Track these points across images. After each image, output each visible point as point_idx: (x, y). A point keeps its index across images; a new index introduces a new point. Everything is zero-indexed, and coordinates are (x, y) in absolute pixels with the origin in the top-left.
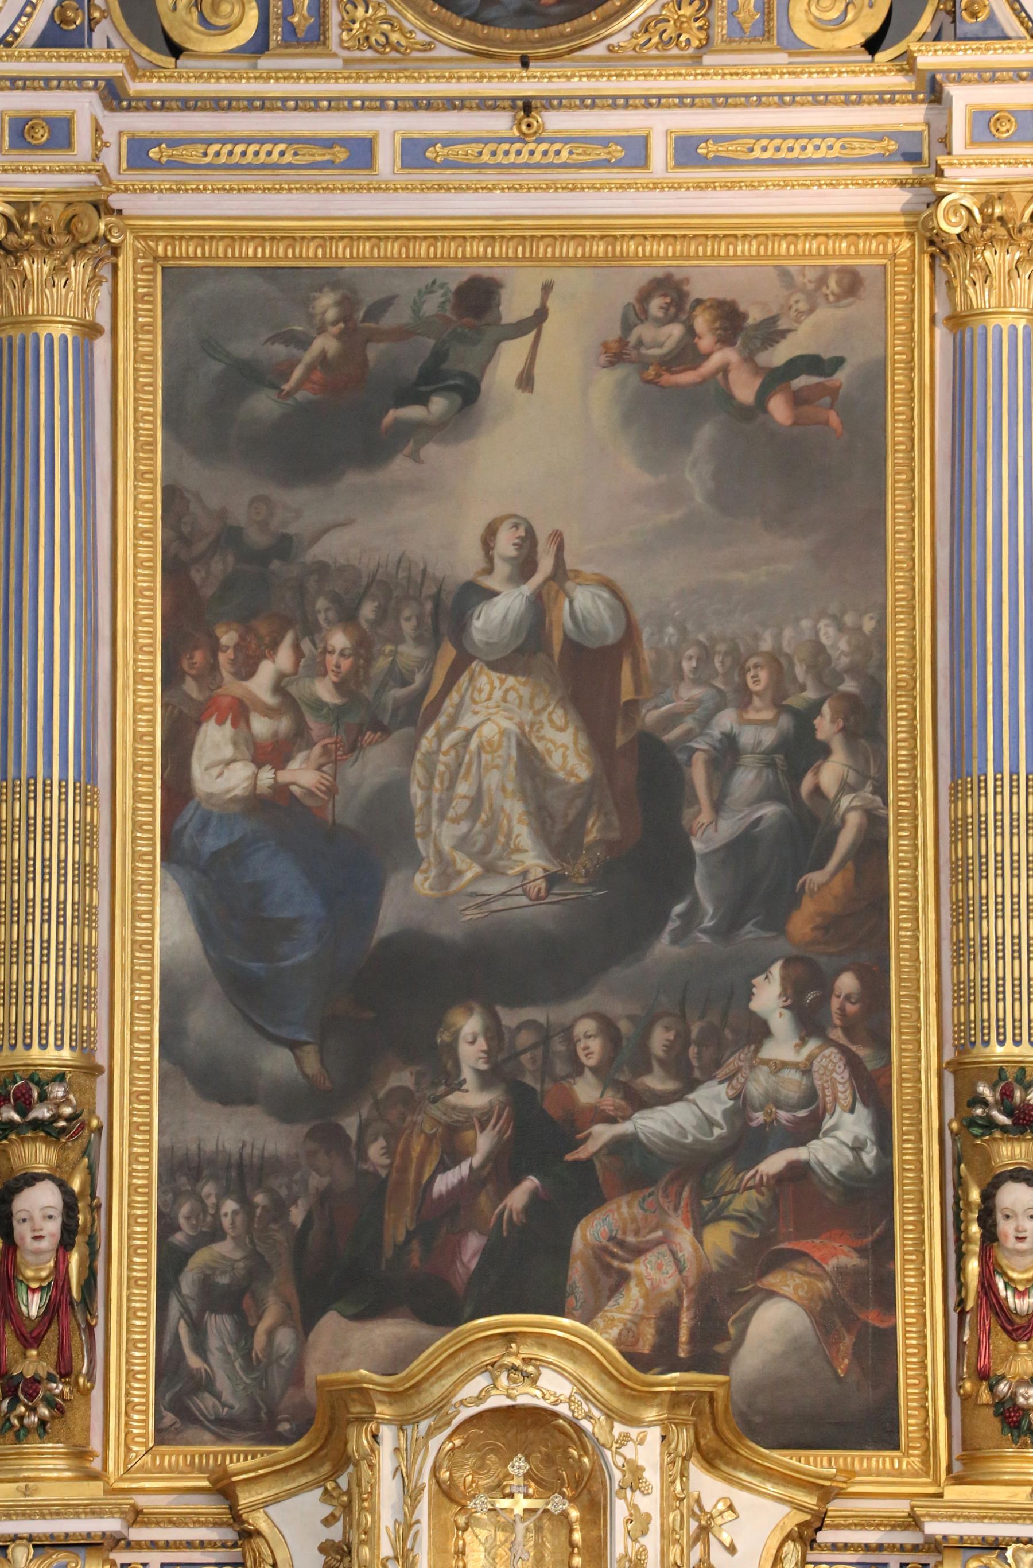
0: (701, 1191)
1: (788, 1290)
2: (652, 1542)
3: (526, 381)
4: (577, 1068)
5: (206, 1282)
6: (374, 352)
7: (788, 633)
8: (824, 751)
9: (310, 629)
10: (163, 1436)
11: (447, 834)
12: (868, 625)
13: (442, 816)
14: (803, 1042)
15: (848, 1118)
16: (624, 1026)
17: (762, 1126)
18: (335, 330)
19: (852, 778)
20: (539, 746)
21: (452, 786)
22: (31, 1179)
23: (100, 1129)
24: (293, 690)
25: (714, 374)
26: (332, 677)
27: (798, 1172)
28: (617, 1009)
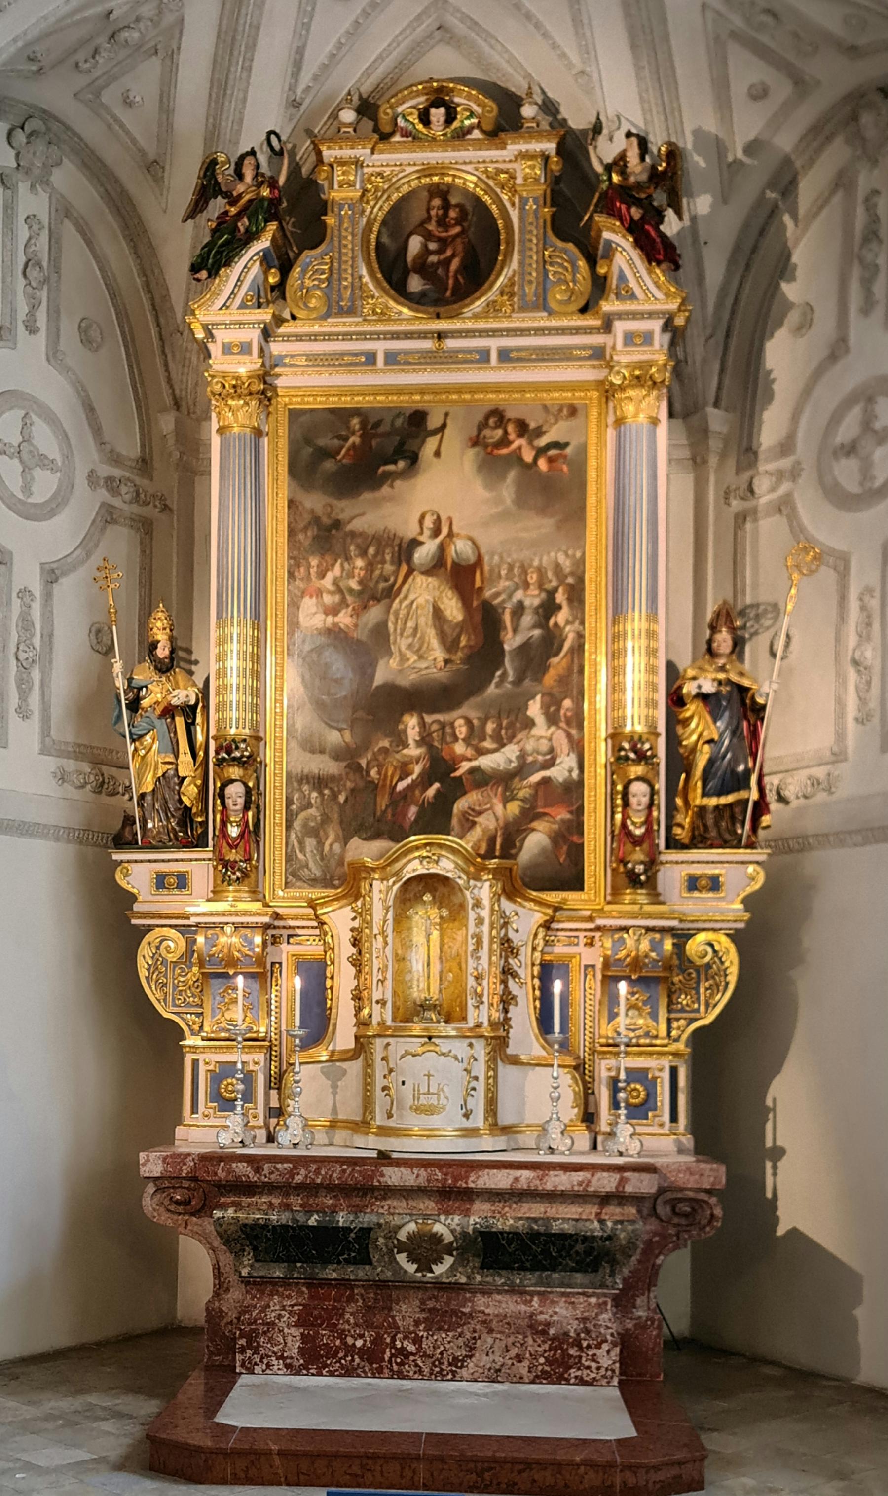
0: (506, 788)
1: (540, 828)
2: (486, 928)
3: (437, 454)
4: (456, 739)
5: (305, 825)
6: (374, 443)
7: (545, 558)
8: (559, 607)
9: (348, 558)
10: (287, 885)
11: (403, 643)
12: (578, 555)
13: (401, 635)
14: (549, 727)
15: (567, 759)
16: (476, 722)
17: (531, 763)
18: (358, 434)
19: (570, 618)
20: (442, 607)
21: (405, 623)
22: (232, 781)
23: (261, 762)
24: (341, 584)
25: (515, 451)
26: (356, 578)
27: (546, 781)
28: (474, 715)
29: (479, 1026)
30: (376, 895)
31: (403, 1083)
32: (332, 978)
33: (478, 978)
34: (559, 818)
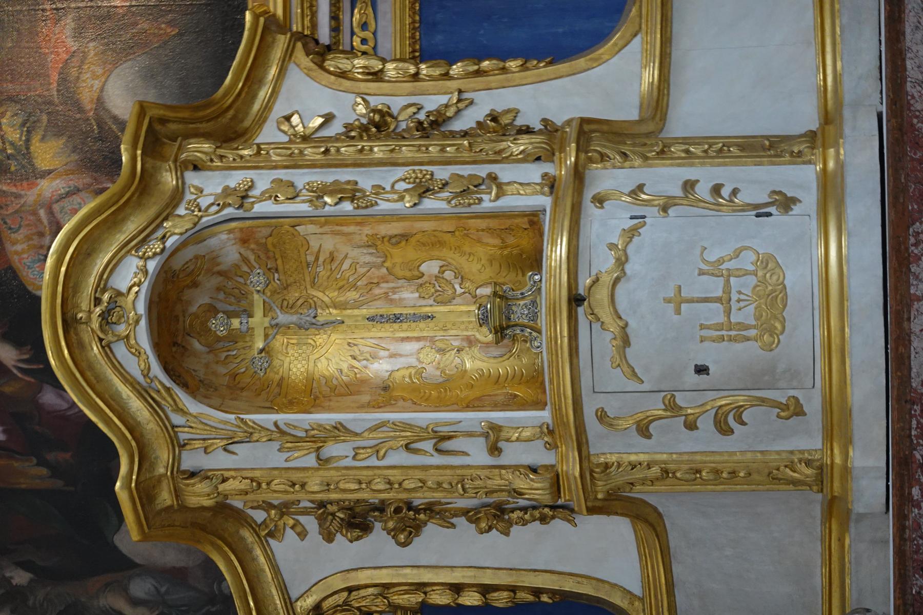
2: (302, 178)
29: (551, 184)
30: (219, 460)
31: (701, 370)
32: (457, 588)
33: (424, 190)
34: (73, 45)
